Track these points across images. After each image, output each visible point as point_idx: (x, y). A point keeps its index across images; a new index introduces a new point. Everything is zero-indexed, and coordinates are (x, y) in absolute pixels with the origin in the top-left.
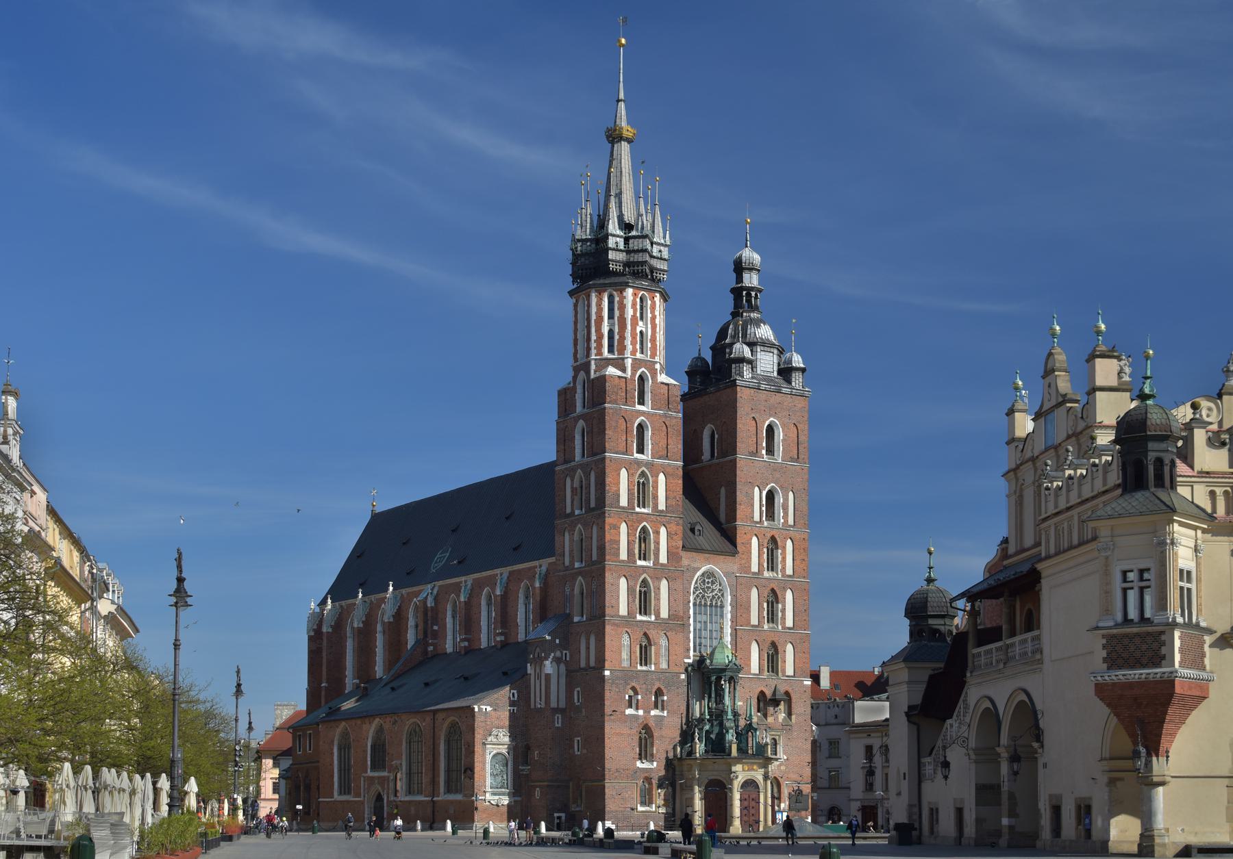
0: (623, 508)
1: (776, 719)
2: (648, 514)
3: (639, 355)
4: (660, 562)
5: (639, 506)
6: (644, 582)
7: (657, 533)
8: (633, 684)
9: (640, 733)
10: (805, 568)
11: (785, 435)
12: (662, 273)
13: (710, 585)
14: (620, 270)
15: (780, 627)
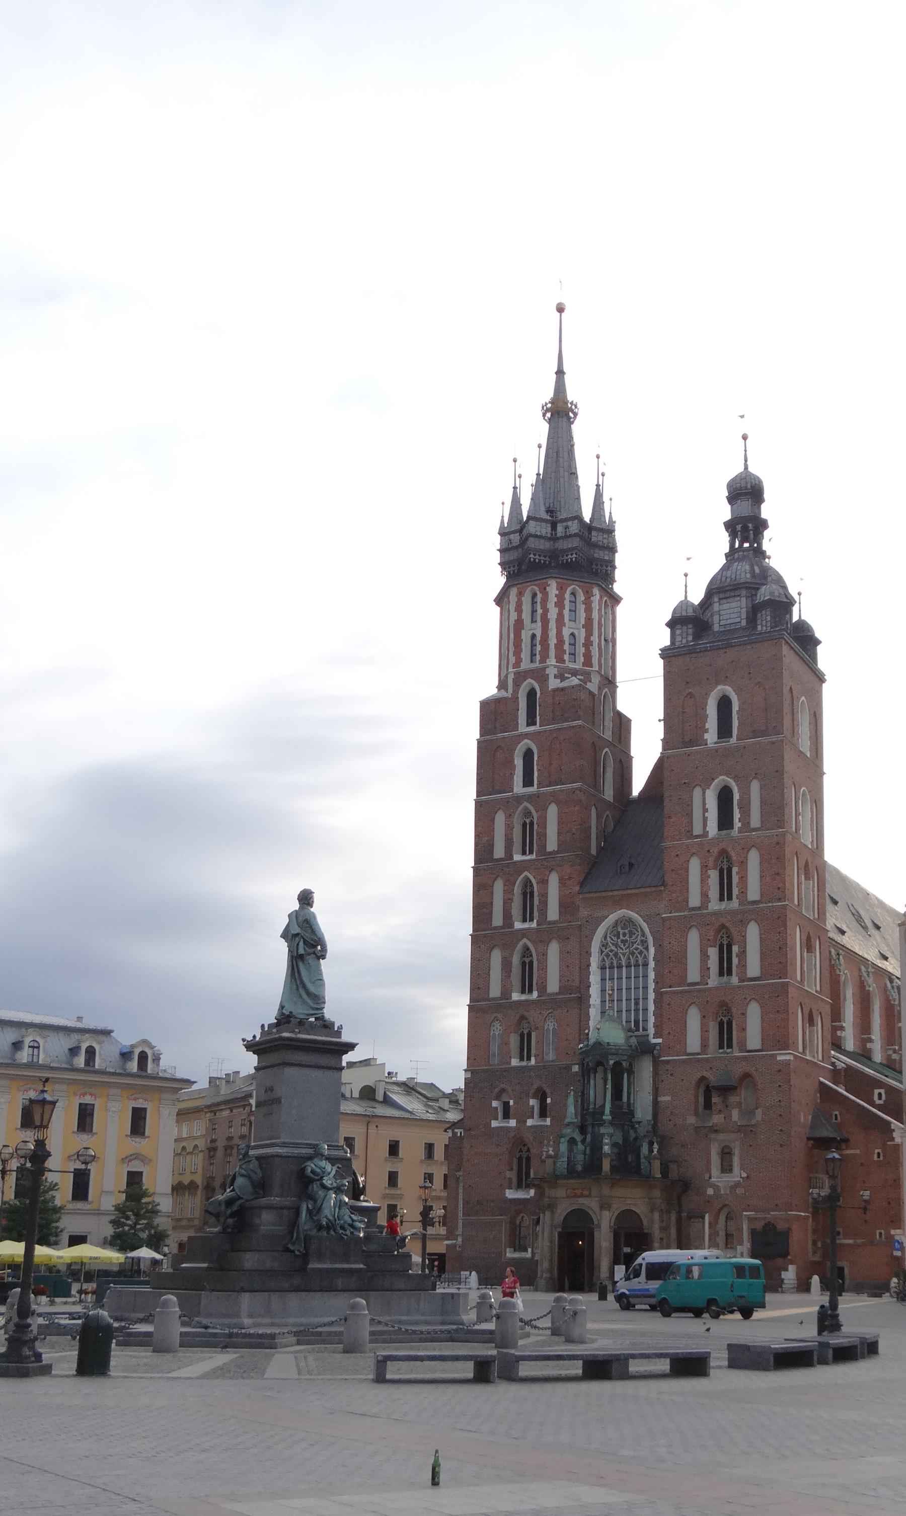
0: (497, 860)
1: (728, 1117)
2: (530, 861)
3: (525, 665)
4: (549, 919)
5: (524, 853)
6: (526, 951)
7: (544, 882)
8: (503, 1086)
9: (521, 1151)
10: (780, 885)
11: (742, 703)
12: (569, 554)
13: (627, 938)
14: (514, 571)
15: (735, 980)
